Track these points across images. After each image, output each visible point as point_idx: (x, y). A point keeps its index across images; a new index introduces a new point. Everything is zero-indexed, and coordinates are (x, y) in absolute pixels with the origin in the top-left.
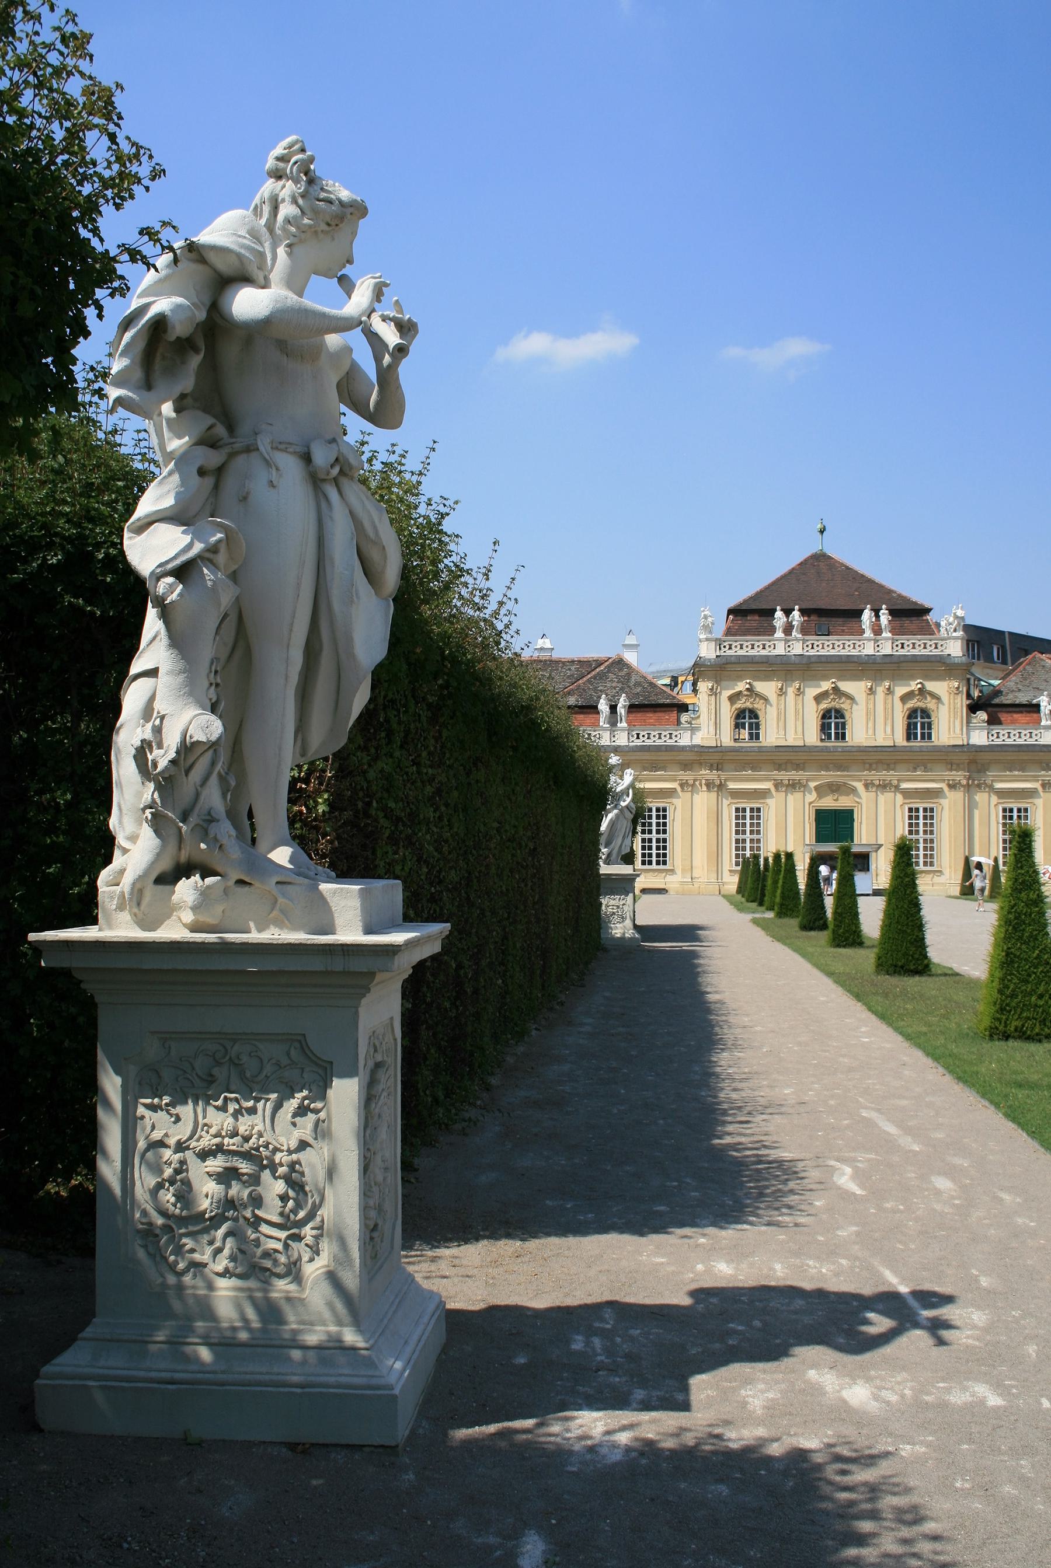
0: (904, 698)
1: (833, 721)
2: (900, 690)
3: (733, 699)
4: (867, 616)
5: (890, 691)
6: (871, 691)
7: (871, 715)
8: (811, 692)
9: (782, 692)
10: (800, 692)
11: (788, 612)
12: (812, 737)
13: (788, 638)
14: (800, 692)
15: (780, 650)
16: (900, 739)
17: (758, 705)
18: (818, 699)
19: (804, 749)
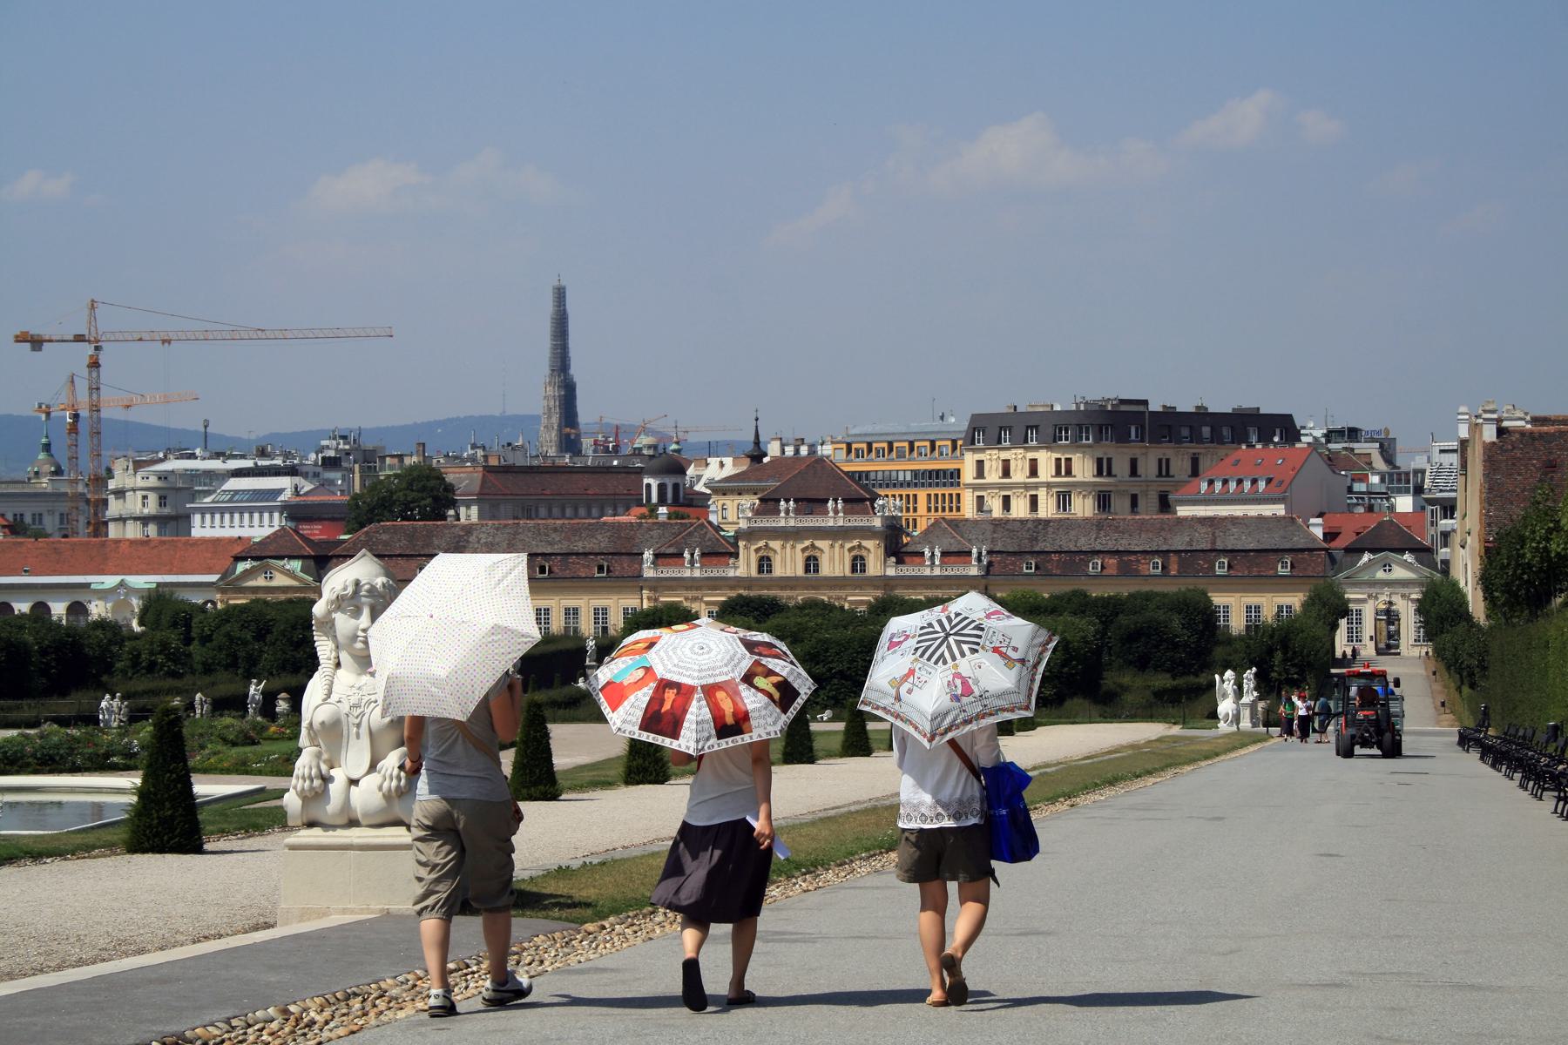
0: (850, 550)
1: (811, 563)
2: (848, 545)
3: (757, 551)
4: (830, 504)
5: (842, 546)
6: (832, 546)
7: (832, 559)
8: (800, 546)
9: (783, 547)
10: (793, 547)
11: (787, 501)
12: (800, 572)
13: (787, 518)
14: (793, 547)
15: (782, 523)
16: (848, 573)
17: (771, 554)
18: (803, 550)
19: (796, 578)
